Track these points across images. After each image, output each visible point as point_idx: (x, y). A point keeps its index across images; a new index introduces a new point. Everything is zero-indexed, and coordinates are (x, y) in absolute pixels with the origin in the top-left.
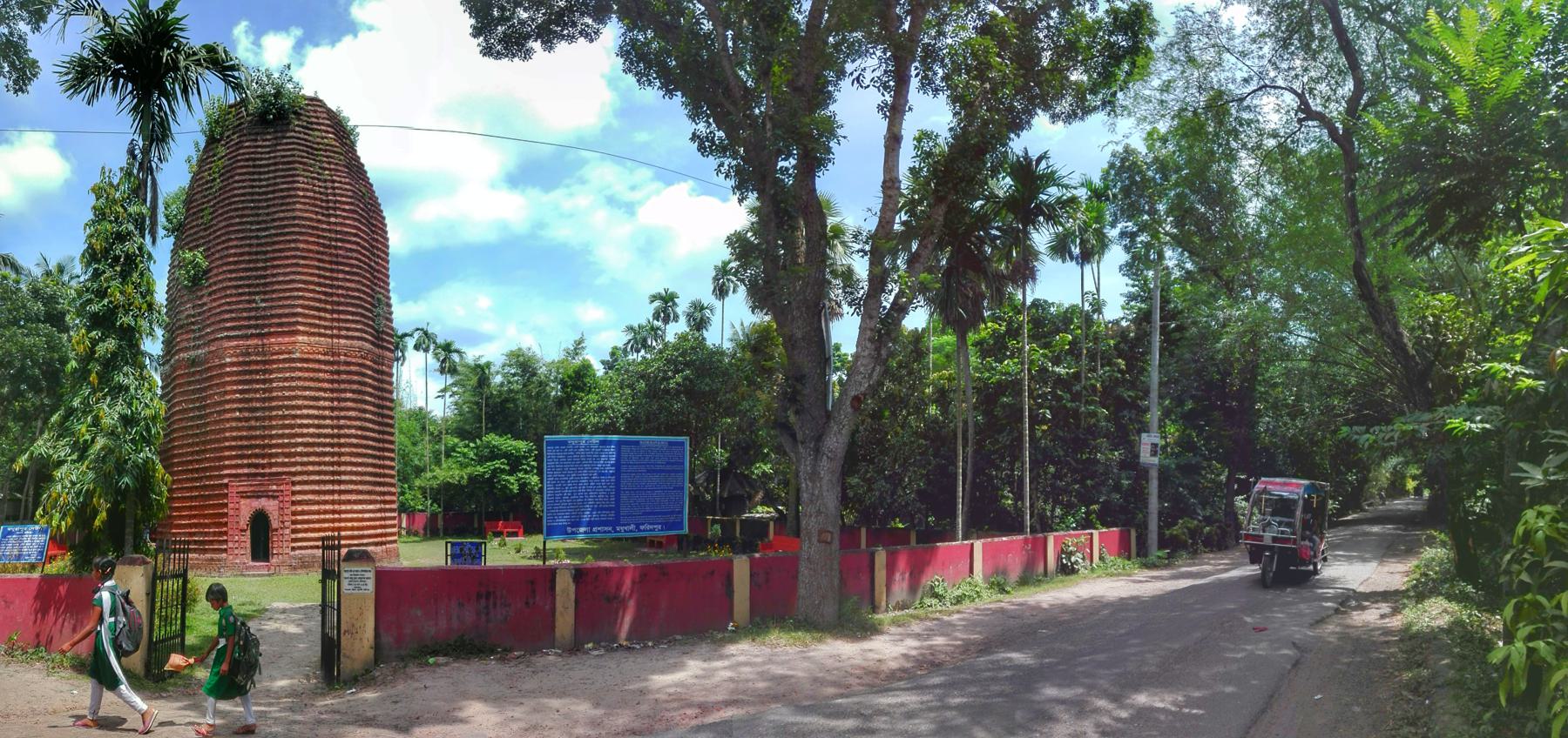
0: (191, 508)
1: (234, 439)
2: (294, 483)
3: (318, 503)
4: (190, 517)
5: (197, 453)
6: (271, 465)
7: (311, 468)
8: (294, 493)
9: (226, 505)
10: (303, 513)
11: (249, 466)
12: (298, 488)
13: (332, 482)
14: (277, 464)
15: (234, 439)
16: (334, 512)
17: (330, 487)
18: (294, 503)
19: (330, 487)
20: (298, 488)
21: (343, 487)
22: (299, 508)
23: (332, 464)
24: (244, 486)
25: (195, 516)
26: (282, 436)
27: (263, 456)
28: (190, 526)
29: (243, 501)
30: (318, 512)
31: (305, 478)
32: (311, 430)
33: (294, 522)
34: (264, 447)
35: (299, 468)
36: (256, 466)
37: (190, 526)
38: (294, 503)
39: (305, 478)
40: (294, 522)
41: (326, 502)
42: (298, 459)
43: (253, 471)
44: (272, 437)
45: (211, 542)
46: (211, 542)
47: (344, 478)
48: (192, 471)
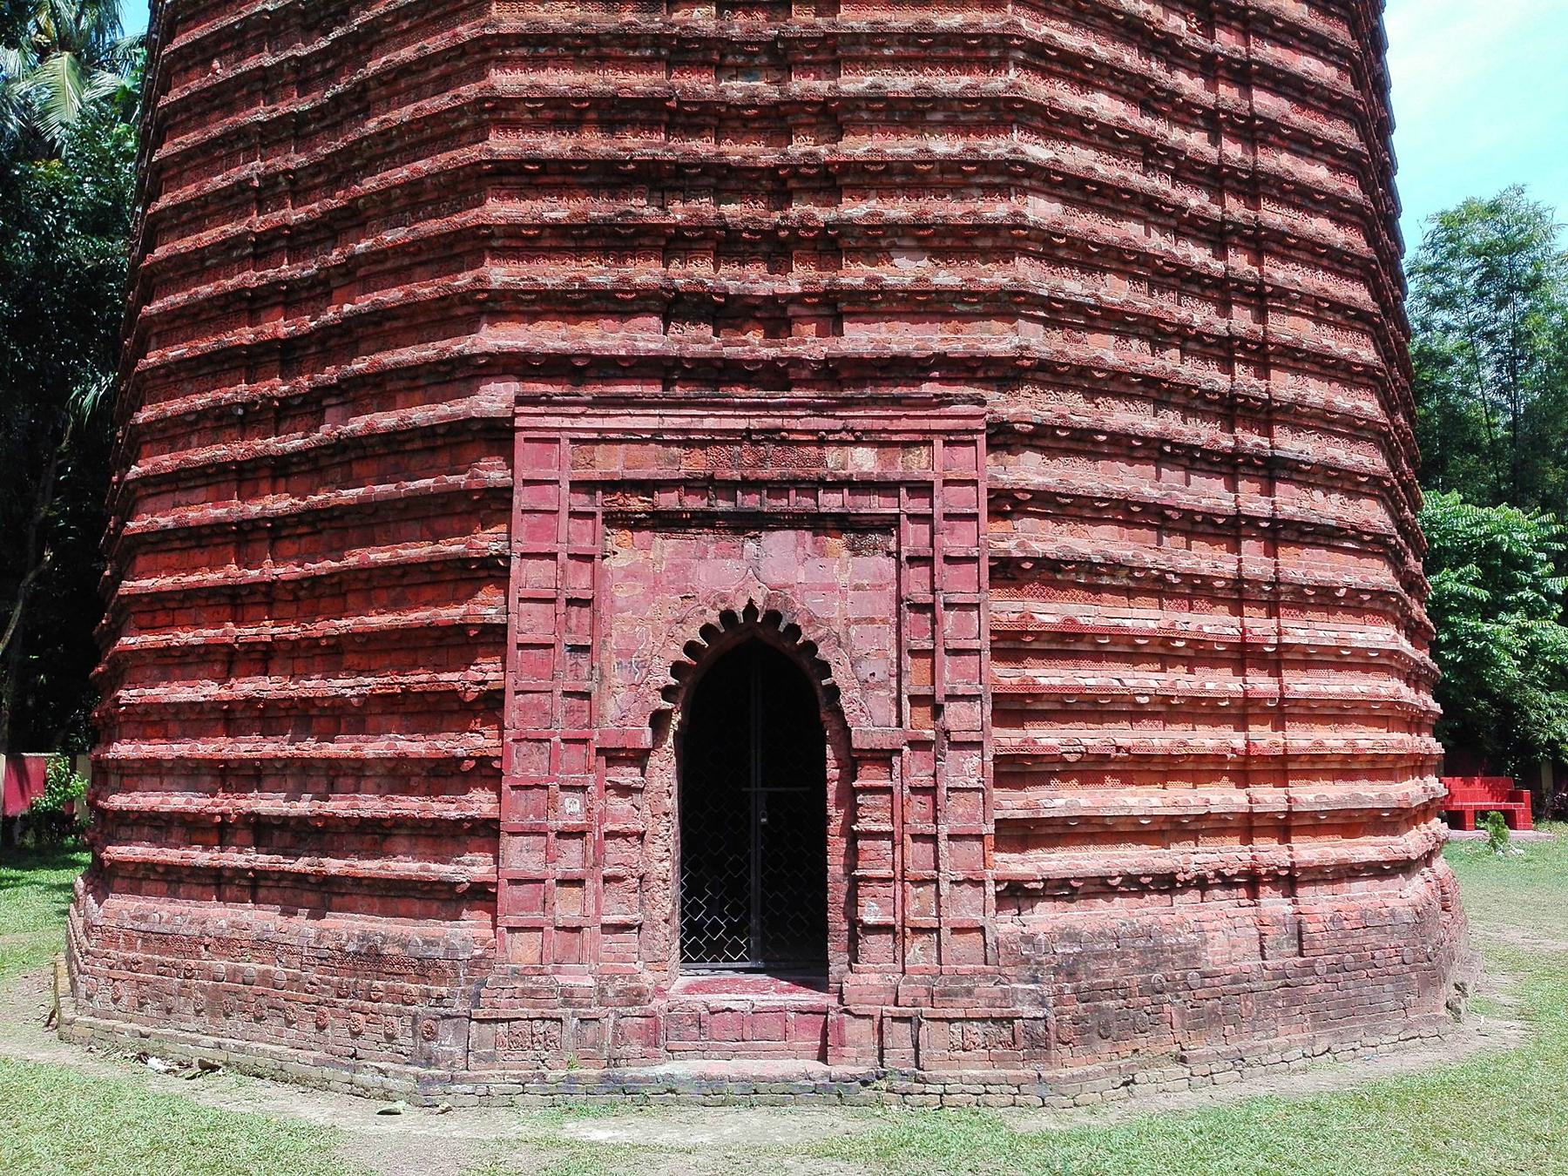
0: (235, 602)
1: (562, 113)
2: (1004, 438)
3: (1157, 587)
4: (230, 660)
5: (296, 241)
6: (834, 309)
7: (1104, 349)
8: (1006, 504)
9: (494, 571)
10: (1067, 644)
11: (674, 306)
12: (1030, 470)
13: (1230, 466)
15: (562, 113)
16: (1243, 655)
17: (1209, 494)
18: (1007, 572)
19: (1209, 494)
20: (1030, 470)
21: (1292, 502)
22: (1050, 612)
23: (1224, 350)
24: (638, 439)
25: (262, 658)
26: (910, 114)
27: (776, 249)
28: (228, 718)
30: (1163, 651)
31: (1073, 408)
32: (1105, 106)
34: (778, 185)
35: (1034, 339)
36: (726, 312)
37: (228, 718)
38: (1007, 572)
39: (1073, 408)
41: (1197, 590)
42: (1028, 273)
43: (697, 341)
44: (834, 117)
45: (375, 835)
46: (375, 835)
47: (1291, 444)
48: (250, 361)
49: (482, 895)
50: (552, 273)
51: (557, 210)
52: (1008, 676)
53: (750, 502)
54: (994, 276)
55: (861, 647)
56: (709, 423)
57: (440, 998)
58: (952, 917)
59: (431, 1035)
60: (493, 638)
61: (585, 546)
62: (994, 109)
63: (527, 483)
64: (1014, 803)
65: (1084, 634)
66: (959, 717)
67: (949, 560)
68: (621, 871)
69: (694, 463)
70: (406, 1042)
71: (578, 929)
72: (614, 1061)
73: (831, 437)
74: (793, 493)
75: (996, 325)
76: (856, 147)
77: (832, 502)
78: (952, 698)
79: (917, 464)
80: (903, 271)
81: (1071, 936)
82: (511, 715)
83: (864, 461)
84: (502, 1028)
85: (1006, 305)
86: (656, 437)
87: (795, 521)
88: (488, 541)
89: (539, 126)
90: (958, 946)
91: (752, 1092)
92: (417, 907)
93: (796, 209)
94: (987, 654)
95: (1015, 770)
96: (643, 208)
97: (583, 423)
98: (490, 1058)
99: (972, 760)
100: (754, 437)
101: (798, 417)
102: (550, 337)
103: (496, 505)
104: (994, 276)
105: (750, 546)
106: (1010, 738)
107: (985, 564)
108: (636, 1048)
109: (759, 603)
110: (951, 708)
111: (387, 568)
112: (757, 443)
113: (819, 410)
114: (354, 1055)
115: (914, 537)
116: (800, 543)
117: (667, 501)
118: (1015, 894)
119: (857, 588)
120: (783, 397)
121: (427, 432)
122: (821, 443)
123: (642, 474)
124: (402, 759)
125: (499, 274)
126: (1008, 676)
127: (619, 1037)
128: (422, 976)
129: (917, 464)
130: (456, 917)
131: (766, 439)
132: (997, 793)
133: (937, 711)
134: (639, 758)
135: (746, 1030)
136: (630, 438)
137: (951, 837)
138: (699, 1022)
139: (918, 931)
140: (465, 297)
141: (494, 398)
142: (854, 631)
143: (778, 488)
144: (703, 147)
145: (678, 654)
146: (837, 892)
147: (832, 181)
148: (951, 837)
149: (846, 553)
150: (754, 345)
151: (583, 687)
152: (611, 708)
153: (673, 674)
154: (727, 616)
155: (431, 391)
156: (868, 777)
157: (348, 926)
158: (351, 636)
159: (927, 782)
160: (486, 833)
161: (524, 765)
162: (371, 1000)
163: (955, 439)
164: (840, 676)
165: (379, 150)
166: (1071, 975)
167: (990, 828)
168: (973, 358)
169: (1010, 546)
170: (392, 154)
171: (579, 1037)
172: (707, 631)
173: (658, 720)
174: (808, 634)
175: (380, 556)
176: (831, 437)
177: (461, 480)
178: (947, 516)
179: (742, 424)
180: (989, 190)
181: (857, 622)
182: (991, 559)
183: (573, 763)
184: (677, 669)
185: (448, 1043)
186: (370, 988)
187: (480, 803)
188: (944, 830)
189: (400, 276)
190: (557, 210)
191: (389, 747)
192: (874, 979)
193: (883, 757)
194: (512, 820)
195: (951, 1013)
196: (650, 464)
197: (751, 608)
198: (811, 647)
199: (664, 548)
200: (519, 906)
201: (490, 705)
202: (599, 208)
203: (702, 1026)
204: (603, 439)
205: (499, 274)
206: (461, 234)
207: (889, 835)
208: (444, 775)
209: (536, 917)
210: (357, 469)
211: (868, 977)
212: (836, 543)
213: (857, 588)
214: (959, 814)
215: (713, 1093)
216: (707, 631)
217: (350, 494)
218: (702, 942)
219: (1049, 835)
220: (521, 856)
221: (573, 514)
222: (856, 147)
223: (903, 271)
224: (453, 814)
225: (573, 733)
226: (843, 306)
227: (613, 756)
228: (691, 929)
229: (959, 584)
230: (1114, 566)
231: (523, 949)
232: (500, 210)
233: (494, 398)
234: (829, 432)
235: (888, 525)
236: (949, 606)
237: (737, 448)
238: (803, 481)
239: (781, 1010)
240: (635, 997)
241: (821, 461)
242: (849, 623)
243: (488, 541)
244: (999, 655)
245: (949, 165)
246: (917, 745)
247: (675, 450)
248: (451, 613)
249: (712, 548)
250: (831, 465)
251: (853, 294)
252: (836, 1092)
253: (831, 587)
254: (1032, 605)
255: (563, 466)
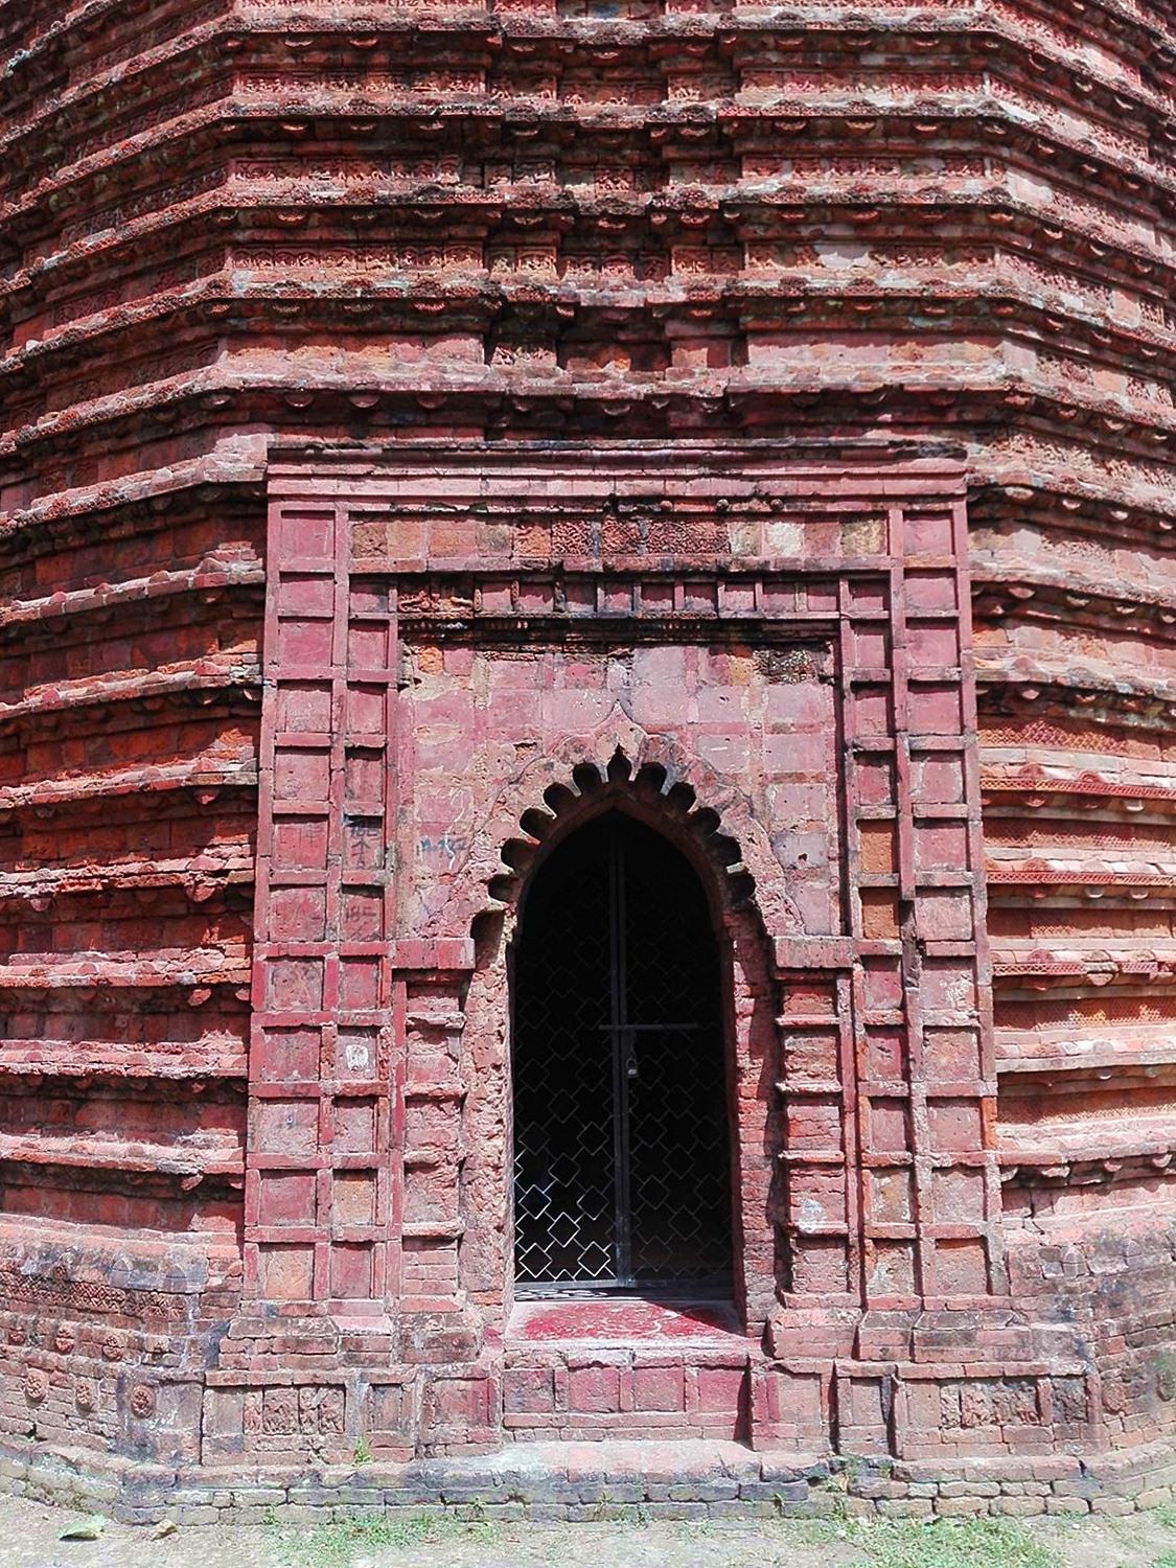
2: (992, 508)
6: (734, 324)
8: (998, 604)
9: (237, 708)
11: (501, 323)
12: (1024, 556)
14: (791, 316)
18: (1003, 705)
20: (1024, 556)
27: (648, 243)
33: (1017, 906)
34: (650, 155)
36: (575, 332)
38: (1003, 705)
40: (1017, 906)
43: (533, 371)
49: (221, 1193)
50: (322, 277)
51: (327, 187)
52: (1008, 858)
53: (616, 604)
54: (969, 278)
55: (784, 817)
56: (555, 488)
57: (158, 1353)
58: (936, 1221)
59: (145, 1409)
60: (236, 806)
61: (372, 670)
62: (957, 50)
63: (286, 576)
65: (1108, 798)
66: (937, 920)
67: (915, 686)
68: (430, 1155)
69: (536, 547)
70: (108, 1416)
71: (367, 1245)
72: (425, 1449)
73: (735, 508)
74: (679, 590)
75: (970, 348)
76: (761, 99)
77: (737, 603)
78: (925, 890)
79: (863, 546)
80: (835, 270)
81: (1111, 1247)
82: (265, 919)
83: (785, 542)
84: (253, 1400)
85: (986, 319)
86: (476, 509)
87: (684, 632)
88: (227, 665)
89: (306, 74)
90: (942, 1265)
91: (646, 1498)
92: (126, 1208)
93: (675, 188)
94: (977, 826)
95: (1025, 999)
96: (453, 184)
97: (368, 488)
98: (237, 1447)
99: (958, 984)
100: (622, 508)
101: (687, 478)
102: (318, 366)
103: (240, 609)
104: (969, 278)
105: (617, 669)
106: (1013, 951)
107: (970, 693)
108: (458, 1427)
109: (632, 753)
110: (924, 907)
111: (83, 708)
112: (626, 517)
113: (717, 467)
114: (33, 1433)
115: (861, 654)
116: (690, 665)
117: (494, 603)
118: (1030, 1184)
119: (776, 729)
120: (665, 448)
121: (142, 508)
122: (722, 516)
123: (457, 564)
124: (103, 987)
125: (244, 278)
126: (1008, 858)
127: (433, 1409)
128: (132, 1317)
129: (863, 546)
130: (183, 1225)
131: (640, 512)
132: (1000, 1034)
133: (903, 910)
134: (455, 983)
135: (622, 1395)
137: (931, 1101)
138: (553, 1383)
139: (883, 1243)
140: (195, 313)
141: (237, 455)
142: (773, 792)
143: (658, 582)
144: (542, 103)
145: (511, 828)
146: (755, 1182)
147: (723, 146)
148: (931, 1101)
149: (759, 679)
150: (616, 379)
151: (372, 877)
152: (413, 911)
153: (505, 859)
154: (585, 773)
155: (147, 452)
156: (800, 1010)
158: (31, 808)
159: (893, 1017)
160: (226, 1098)
161: (284, 996)
162: (56, 1349)
163: (920, 509)
164: (753, 860)
165: (80, 128)
166: (1115, 1307)
167: (990, 1087)
168: (943, 392)
169: (1004, 666)
170: (96, 133)
171: (372, 1414)
172: (554, 794)
173: (483, 927)
174: (705, 798)
175: (72, 692)
176: (735, 508)
177: (190, 576)
178: (911, 622)
179: (603, 489)
180: (954, 160)
181: (777, 779)
182: (979, 684)
183: (357, 994)
184: (511, 851)
185: (170, 1423)
186: (56, 1332)
187: (218, 1053)
188: (921, 1090)
189: (107, 294)
190: (327, 187)
191: (83, 971)
192: (819, 1317)
193: (822, 981)
194: (265, 1079)
195: (941, 1370)
196: (466, 548)
197: (619, 761)
198: (710, 817)
199: (489, 675)
200: (278, 1210)
201: (233, 906)
202: (392, 185)
203: (558, 1390)
204: (399, 512)
205: (244, 278)
207: (836, 1098)
208: (164, 1011)
209: (303, 1226)
210: (42, 569)
211: (812, 1314)
212: (744, 665)
213: (776, 729)
215: (579, 1498)
216: (554, 794)
218: (543, 1252)
219: (1069, 1095)
220: (280, 1134)
221: (355, 624)
222: (761, 99)
223: (835, 270)
224: (176, 1069)
225: (357, 947)
226: (748, 321)
227: (417, 981)
228: (529, 1231)
229: (931, 721)
231: (284, 1276)
232: (245, 188)
233: (237, 455)
234: (733, 499)
235: (822, 636)
236: (917, 754)
237: (597, 526)
238: (696, 572)
239: (677, 1364)
240: (457, 1347)
241: (720, 543)
242: (765, 781)
243: (227, 665)
244: (996, 827)
245: (897, 123)
246: (875, 961)
247: (505, 529)
248: (176, 772)
249: (560, 673)
250: (736, 549)
251: (763, 302)
252: (773, 1496)
253: (737, 729)
254: (1038, 753)
255: (340, 550)
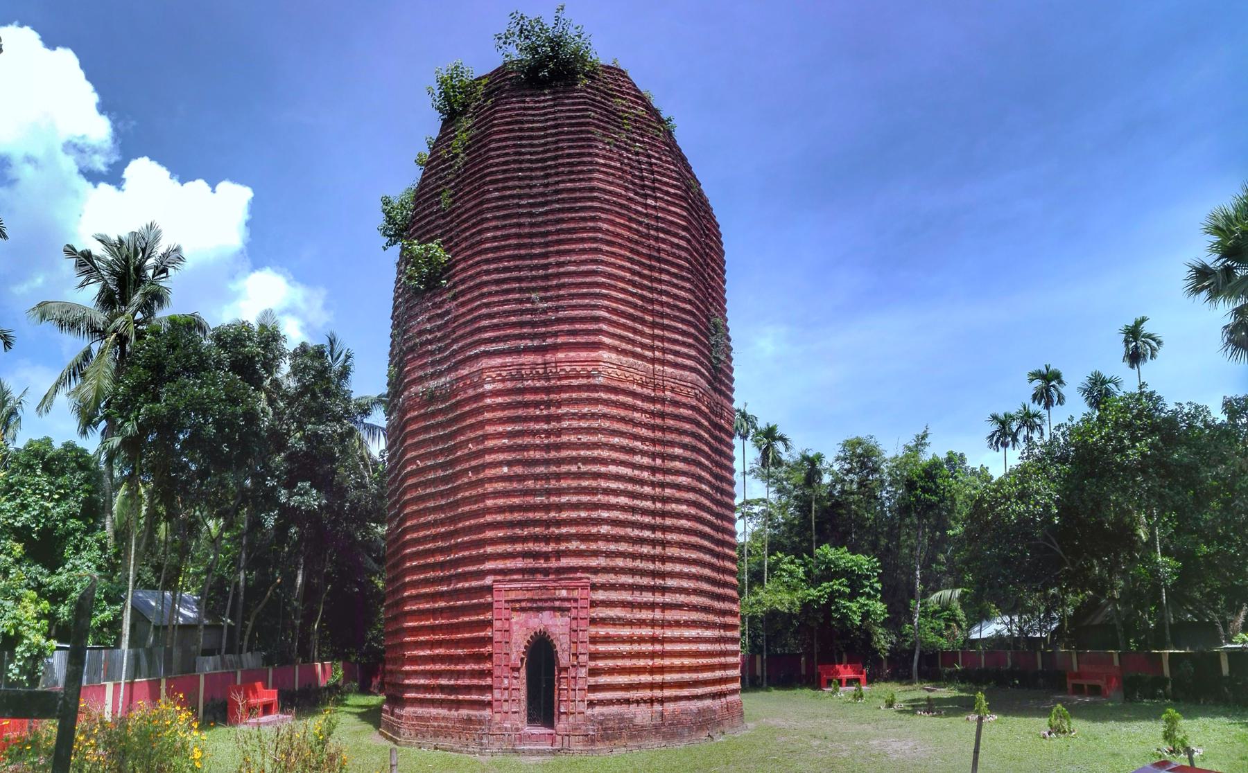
2: (594, 587)
6: (559, 555)
8: (594, 604)
9: (489, 623)
10: (607, 639)
12: (600, 595)
15: (501, 510)
18: (593, 622)
20: (600, 595)
22: (602, 631)
27: (547, 539)
29: (516, 618)
33: (594, 656)
34: (547, 524)
36: (536, 556)
38: (593, 622)
40: (594, 656)
43: (530, 563)
44: (560, 507)
45: (468, 689)
46: (468, 689)
50: (500, 549)
52: (592, 648)
53: (540, 604)
54: (593, 546)
64: (592, 681)
69: (528, 595)
76: (564, 515)
77: (557, 604)
79: (575, 594)
80: (573, 545)
83: (564, 593)
88: (489, 616)
90: (580, 717)
93: (552, 530)
95: (594, 672)
102: (500, 565)
104: (593, 546)
106: (592, 664)
115: (574, 612)
117: (524, 604)
118: (591, 704)
121: (475, 588)
123: (520, 598)
124: (474, 670)
125: (489, 550)
126: (592, 648)
129: (575, 594)
134: (518, 670)
135: (538, 738)
136: (516, 589)
140: (482, 555)
141: (488, 580)
143: (546, 601)
147: (559, 523)
150: (542, 564)
152: (513, 657)
157: (464, 712)
160: (489, 688)
161: (497, 672)
163: (583, 588)
164: (558, 648)
173: (522, 660)
175: (466, 619)
180: (593, 525)
187: (489, 681)
193: (566, 669)
199: (523, 616)
202: (509, 533)
204: (511, 590)
205: (489, 550)
206: (481, 540)
211: (561, 725)
214: (581, 684)
217: (459, 603)
222: (564, 515)
223: (573, 545)
229: (583, 625)
230: (619, 618)
233: (488, 580)
235: (569, 609)
240: (517, 729)
243: (489, 616)
244: (591, 642)
245: (584, 519)
246: (573, 666)
248: (482, 634)
255: (503, 597)
